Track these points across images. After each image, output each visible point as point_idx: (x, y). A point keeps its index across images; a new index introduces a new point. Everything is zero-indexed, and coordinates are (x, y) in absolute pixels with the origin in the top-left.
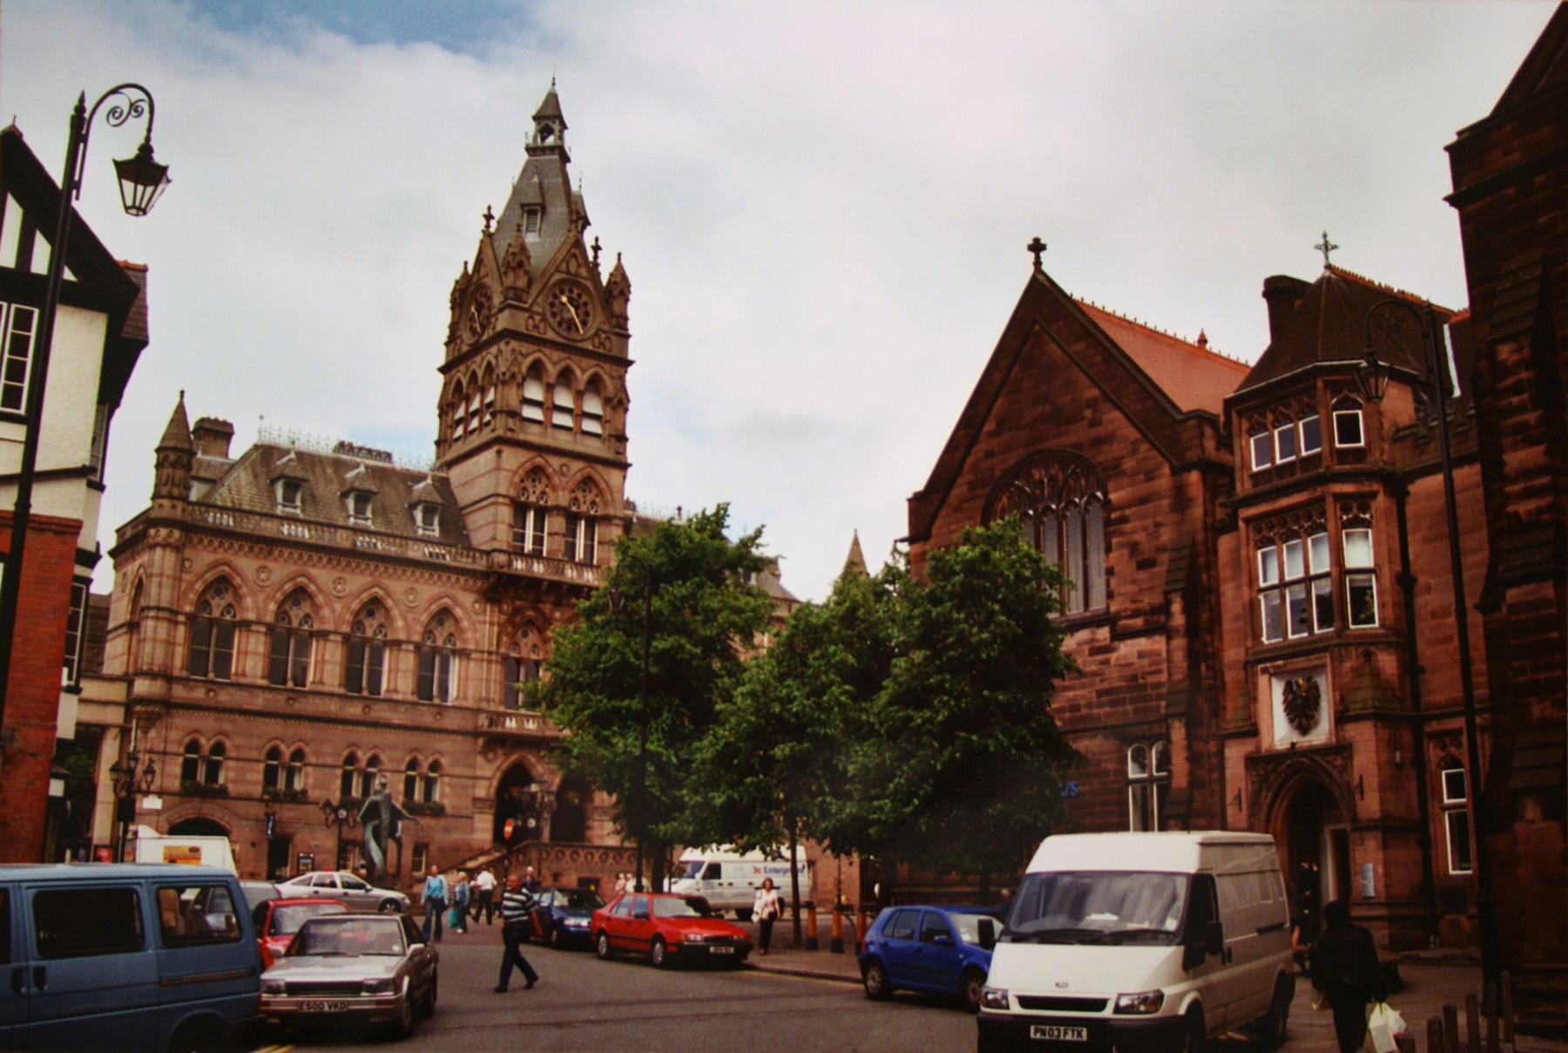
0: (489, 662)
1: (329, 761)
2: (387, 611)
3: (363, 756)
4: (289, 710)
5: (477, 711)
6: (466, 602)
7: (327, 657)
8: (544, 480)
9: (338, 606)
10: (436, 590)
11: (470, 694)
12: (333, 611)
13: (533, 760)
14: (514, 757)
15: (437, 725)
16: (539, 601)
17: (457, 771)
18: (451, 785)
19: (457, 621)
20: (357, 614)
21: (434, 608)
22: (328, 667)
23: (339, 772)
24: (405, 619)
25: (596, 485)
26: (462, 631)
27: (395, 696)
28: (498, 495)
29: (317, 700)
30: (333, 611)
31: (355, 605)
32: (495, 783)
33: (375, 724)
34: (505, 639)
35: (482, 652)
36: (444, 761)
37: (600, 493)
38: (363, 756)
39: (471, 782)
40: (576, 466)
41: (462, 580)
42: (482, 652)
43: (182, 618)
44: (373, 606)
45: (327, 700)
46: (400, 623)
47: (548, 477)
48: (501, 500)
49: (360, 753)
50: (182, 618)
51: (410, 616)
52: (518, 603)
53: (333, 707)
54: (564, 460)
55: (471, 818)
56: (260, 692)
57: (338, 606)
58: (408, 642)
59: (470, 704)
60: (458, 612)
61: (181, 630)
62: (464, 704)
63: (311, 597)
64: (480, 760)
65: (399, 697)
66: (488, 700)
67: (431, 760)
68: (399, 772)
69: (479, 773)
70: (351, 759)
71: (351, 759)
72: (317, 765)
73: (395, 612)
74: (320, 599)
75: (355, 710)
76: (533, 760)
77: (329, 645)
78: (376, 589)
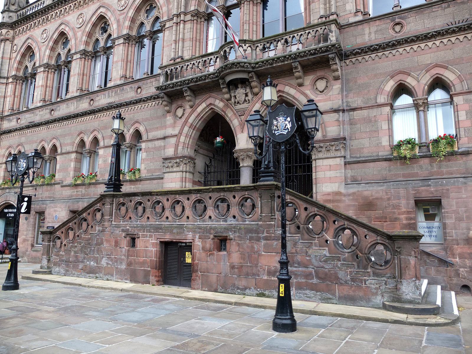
3: (88, 140)
15: (139, 97)
17: (151, 135)
18: (147, 150)
20: (90, 35)
38: (88, 140)
39: (161, 143)
43: (10, 80)
49: (86, 139)
50: (10, 80)
56: (37, 112)
61: (10, 87)
64: (169, 119)
70: (82, 143)
71: (82, 143)
73: (112, 19)
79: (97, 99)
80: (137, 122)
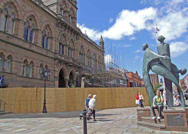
0: (57, 41)
1: (20, 60)
2: (35, 20)
3: (29, 61)
4: (7, 41)
5: (55, 53)
6: (53, 25)
7: (20, 27)
8: (65, 5)
9: (23, 13)
10: (47, 19)
11: (54, 49)
12: (22, 14)
13: (65, 68)
14: (62, 67)
15: (46, 55)
16: (65, 30)
19: (50, 29)
21: (46, 23)
22: (20, 30)
23: (23, 65)
24: (40, 24)
25: (73, 10)
26: (51, 32)
27: (37, 45)
28: (58, 3)
29: (16, 40)
30: (22, 14)
31: (28, 15)
32: (59, 73)
33: (33, 51)
34: (60, 37)
35: (56, 39)
36: (48, 65)
37: (73, 12)
38: (29, 61)
40: (70, 4)
41: (52, 19)
42: (56, 39)
44: (32, 18)
45: (19, 41)
46: (38, 24)
47: (66, 4)
48: (58, 4)
49: (28, 60)
51: (41, 24)
52: (62, 29)
53: (21, 43)
54: (69, 2)
55: (54, 82)
57: (23, 13)
58: (41, 30)
59: (53, 51)
60: (51, 27)
62: (52, 51)
63: (15, 7)
65: (38, 45)
66: (57, 51)
67: (45, 65)
68: (38, 67)
69: (56, 70)
70: (25, 61)
71: (25, 61)
72: (16, 61)
73: (37, 21)
74: (18, 9)
75: (27, 46)
76: (65, 68)
77: (20, 24)
78: (33, 13)
79: (33, 47)
80: (47, 63)
